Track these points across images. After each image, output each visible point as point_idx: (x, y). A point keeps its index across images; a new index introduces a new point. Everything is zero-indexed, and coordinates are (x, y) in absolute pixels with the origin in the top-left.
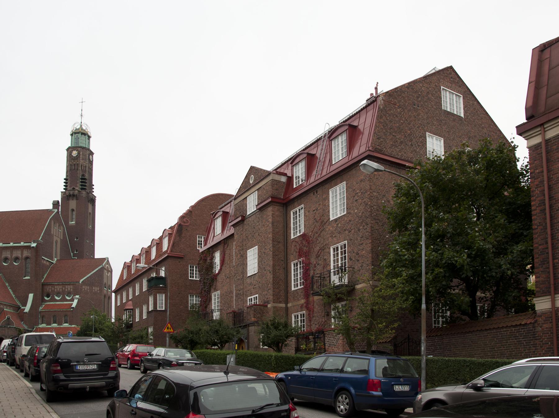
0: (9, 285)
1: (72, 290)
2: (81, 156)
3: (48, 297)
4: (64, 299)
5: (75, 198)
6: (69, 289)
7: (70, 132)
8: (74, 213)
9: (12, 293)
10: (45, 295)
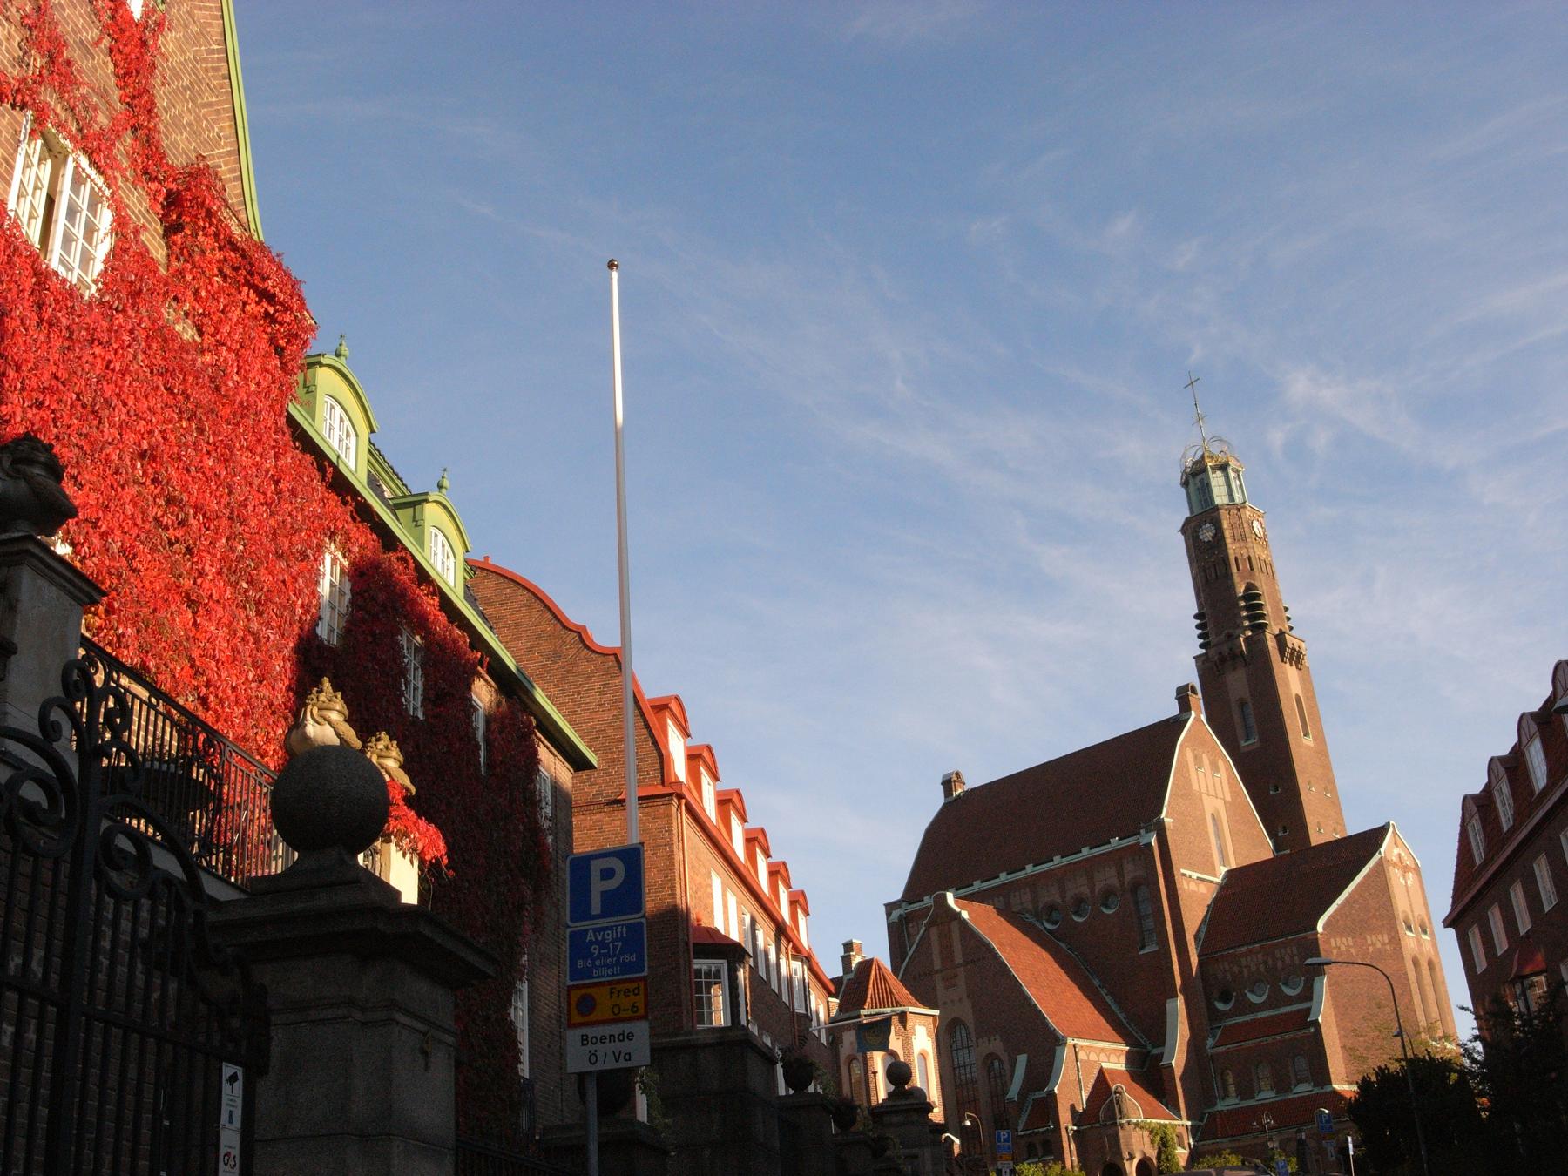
2: (1227, 534)
3: (1226, 1001)
6: (1288, 960)
7: (1176, 478)
8: (1250, 710)
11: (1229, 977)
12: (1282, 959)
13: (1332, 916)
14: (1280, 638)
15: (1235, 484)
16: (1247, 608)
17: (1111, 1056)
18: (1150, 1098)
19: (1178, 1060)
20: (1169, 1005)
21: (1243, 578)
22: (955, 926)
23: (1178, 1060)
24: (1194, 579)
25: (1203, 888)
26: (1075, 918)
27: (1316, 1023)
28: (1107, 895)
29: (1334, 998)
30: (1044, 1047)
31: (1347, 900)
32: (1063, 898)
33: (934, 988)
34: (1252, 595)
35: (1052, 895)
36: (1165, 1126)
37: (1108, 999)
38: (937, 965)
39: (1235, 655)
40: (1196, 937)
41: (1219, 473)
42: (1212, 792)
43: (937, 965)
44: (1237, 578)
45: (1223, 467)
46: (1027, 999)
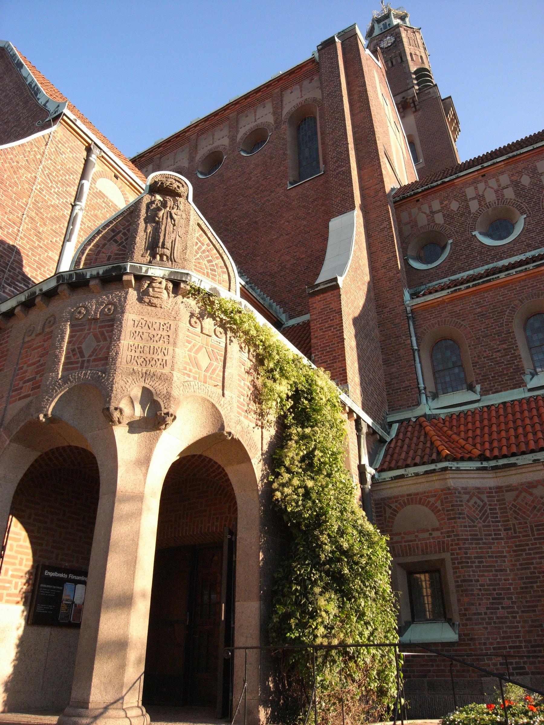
2: (405, 40)
11: (439, 219)
16: (417, 79)
20: (334, 224)
21: (415, 64)
26: (200, 176)
28: (257, 139)
44: (410, 63)
45: (403, 18)
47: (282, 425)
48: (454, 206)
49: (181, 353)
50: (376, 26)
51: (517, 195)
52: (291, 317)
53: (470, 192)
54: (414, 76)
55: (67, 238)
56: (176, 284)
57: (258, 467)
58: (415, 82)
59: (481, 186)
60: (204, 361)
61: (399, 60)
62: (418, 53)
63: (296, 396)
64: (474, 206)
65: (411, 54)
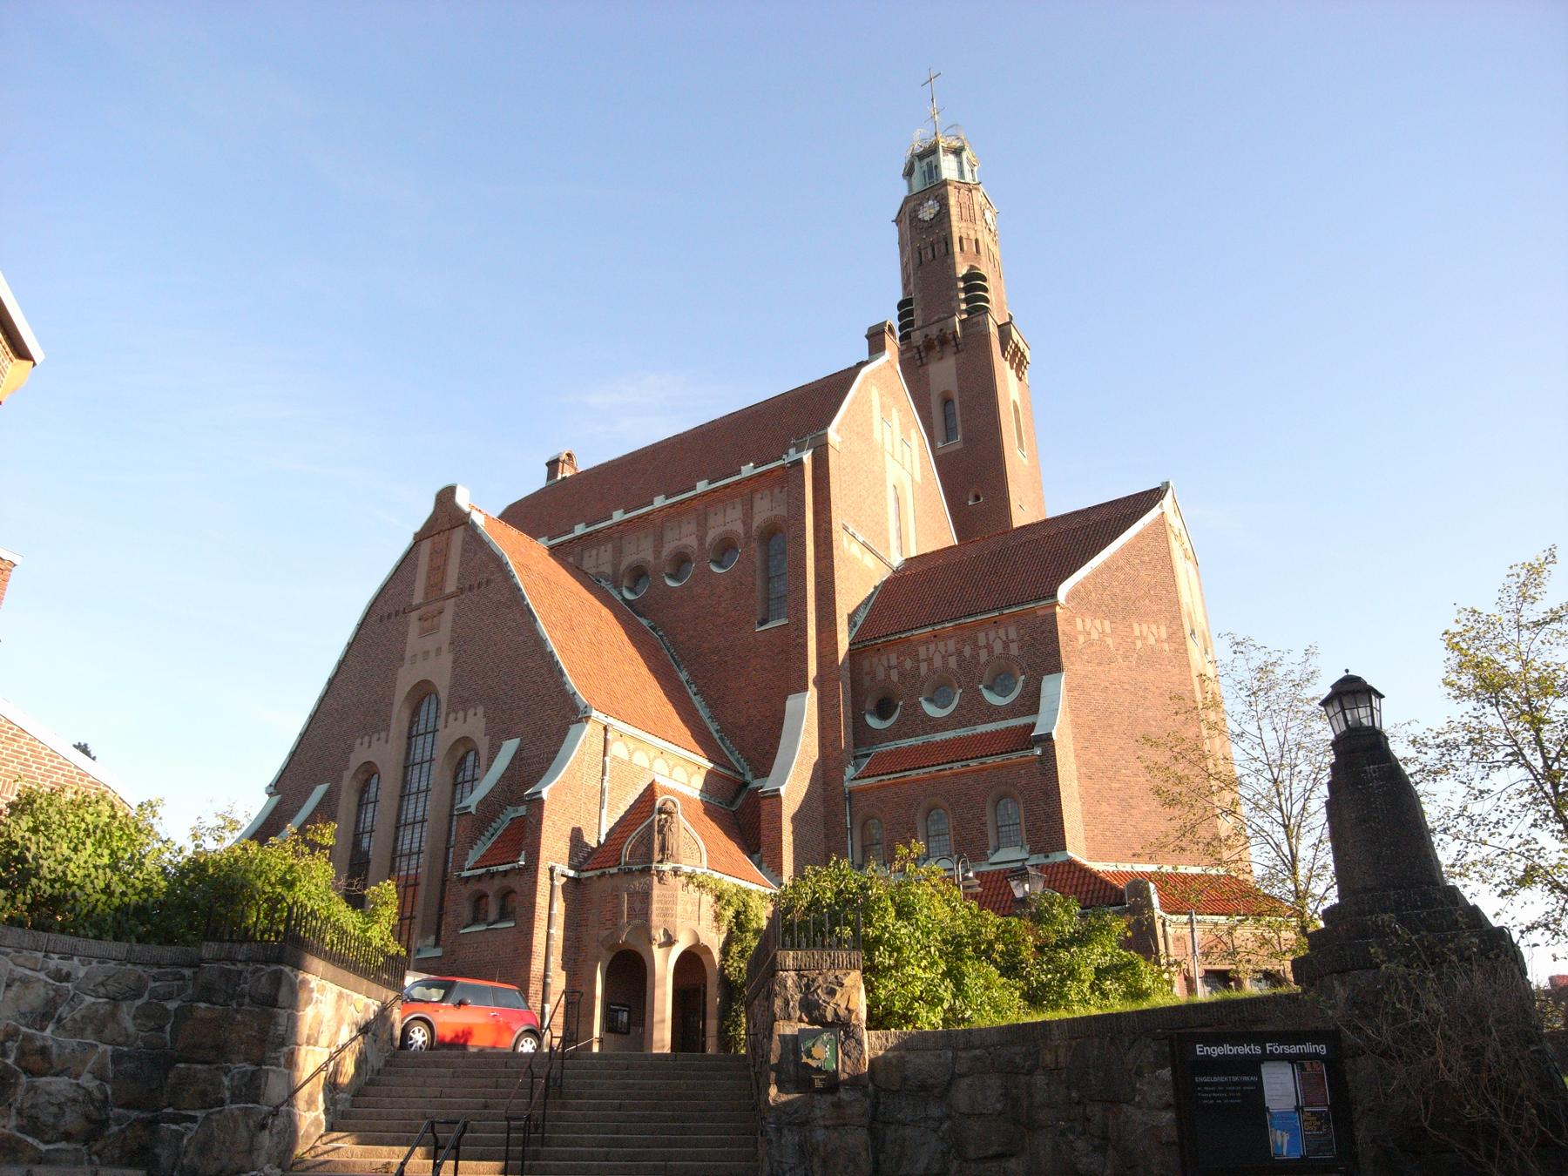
0: (694, 679)
1: (1014, 650)
2: (954, 211)
3: (883, 713)
4: (974, 710)
5: (950, 349)
6: (998, 648)
9: (704, 713)
10: (870, 704)
11: (894, 675)
12: (989, 648)
13: (1082, 583)
14: (1004, 330)
15: (966, 168)
16: (966, 290)
17: (682, 773)
18: (732, 847)
19: (793, 785)
20: (791, 703)
21: (966, 259)
22: (458, 535)
23: (793, 785)
24: (904, 268)
25: (869, 560)
27: (1047, 740)
28: (725, 547)
29: (1073, 711)
30: (545, 715)
31: (1106, 566)
32: (657, 553)
33: (404, 634)
34: (975, 281)
35: (641, 551)
36: (748, 893)
37: (697, 701)
38: (418, 598)
39: (944, 340)
40: (851, 617)
41: (951, 157)
42: (898, 456)
43: (418, 598)
44: (958, 257)
45: (957, 152)
46: (540, 642)
47: (730, 931)
48: (908, 664)
49: (679, 908)
50: (917, 165)
51: (959, 666)
52: (756, 777)
53: (922, 651)
54: (961, 285)
55: (601, 808)
56: (676, 872)
57: (717, 956)
58: (962, 296)
59: (932, 647)
60: (689, 908)
61: (943, 250)
62: (972, 233)
63: (738, 914)
64: (924, 667)
65: (961, 239)
